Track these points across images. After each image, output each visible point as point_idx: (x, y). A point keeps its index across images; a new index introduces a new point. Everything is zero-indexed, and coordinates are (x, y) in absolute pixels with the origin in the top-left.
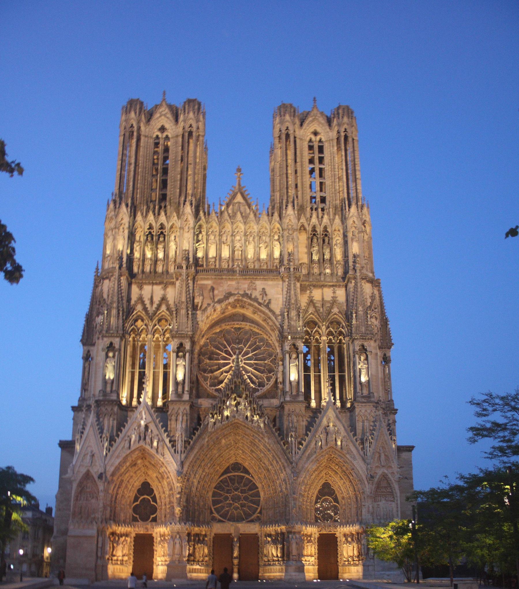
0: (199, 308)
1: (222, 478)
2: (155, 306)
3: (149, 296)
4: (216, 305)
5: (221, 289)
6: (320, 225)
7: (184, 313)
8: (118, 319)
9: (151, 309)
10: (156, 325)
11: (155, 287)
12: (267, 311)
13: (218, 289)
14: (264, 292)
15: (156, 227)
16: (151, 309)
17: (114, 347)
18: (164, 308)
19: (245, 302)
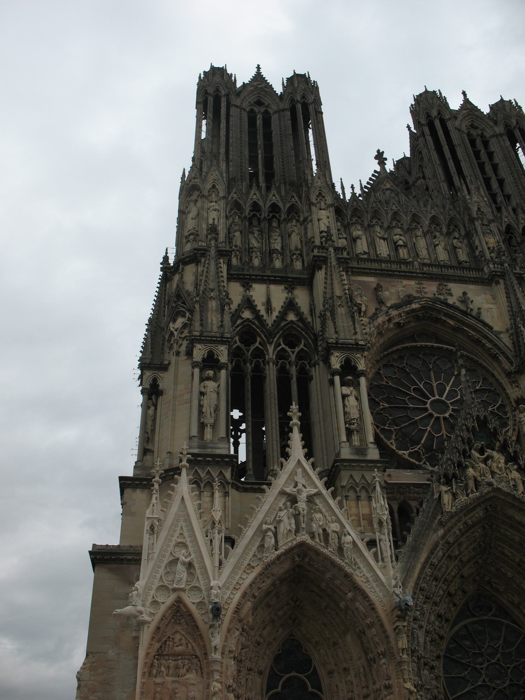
1: (457, 628)
2: (275, 314)
3: (264, 300)
4: (390, 311)
5: (393, 290)
6: (518, 225)
7: (343, 312)
8: (222, 316)
9: (270, 320)
10: (280, 345)
11: (273, 287)
13: (387, 290)
14: (464, 299)
15: (265, 207)
16: (270, 320)
17: (218, 361)
18: (291, 317)
19: (439, 311)
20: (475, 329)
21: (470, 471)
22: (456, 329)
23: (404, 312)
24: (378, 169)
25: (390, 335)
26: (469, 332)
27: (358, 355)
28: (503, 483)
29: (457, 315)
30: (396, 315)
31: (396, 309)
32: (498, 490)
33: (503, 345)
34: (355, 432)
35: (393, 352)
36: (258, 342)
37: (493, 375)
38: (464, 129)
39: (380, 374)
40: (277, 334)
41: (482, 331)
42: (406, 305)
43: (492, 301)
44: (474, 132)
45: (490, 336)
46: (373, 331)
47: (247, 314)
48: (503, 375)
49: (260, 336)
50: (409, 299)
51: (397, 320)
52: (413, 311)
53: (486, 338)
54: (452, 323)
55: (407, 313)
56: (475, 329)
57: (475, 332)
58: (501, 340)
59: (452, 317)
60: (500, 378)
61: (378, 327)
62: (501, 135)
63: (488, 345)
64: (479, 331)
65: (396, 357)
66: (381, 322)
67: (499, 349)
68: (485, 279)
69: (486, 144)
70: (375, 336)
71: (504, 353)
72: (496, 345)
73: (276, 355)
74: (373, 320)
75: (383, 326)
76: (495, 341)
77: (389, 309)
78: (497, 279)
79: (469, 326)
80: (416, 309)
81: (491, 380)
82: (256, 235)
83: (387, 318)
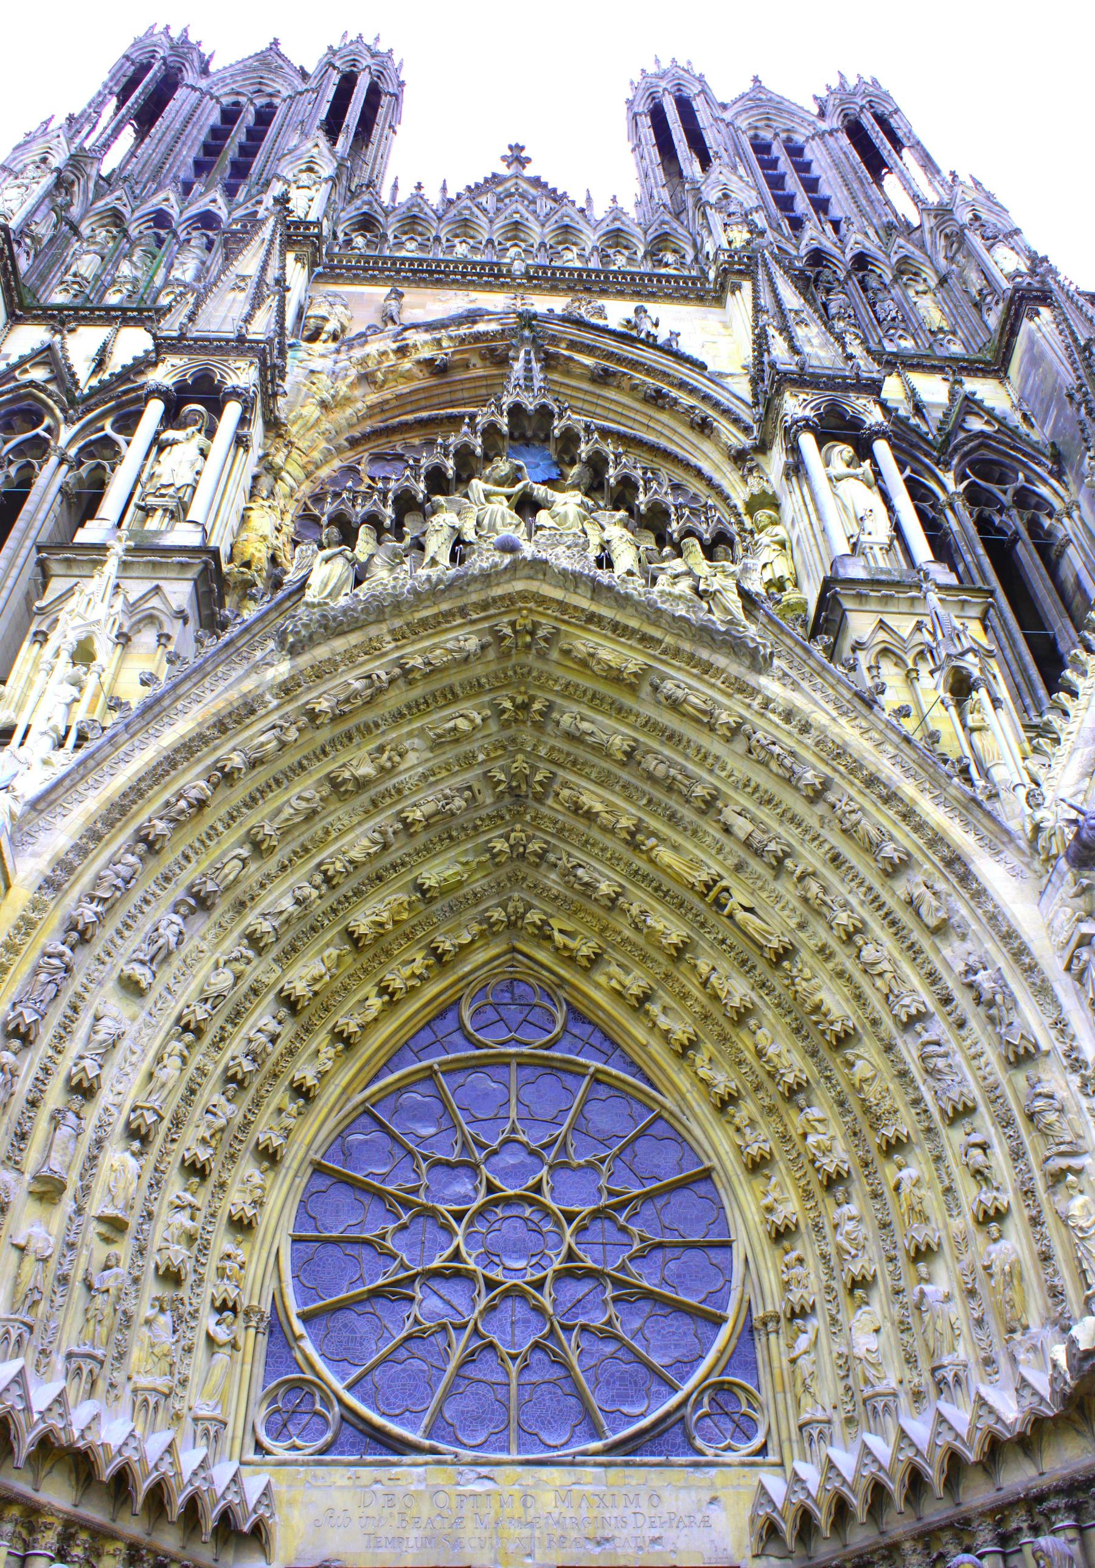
0: (324, 336)
12: (666, 363)
20: (650, 371)
21: (445, 519)
22: (602, 378)
23: (450, 338)
24: (503, 170)
25: (404, 388)
26: (631, 378)
27: (238, 364)
28: (560, 549)
29: (606, 344)
30: (426, 342)
31: (426, 331)
32: (539, 566)
33: (727, 395)
34: (160, 512)
35: (405, 427)
36: (43, 426)
37: (699, 473)
38: (743, 123)
39: (358, 472)
40: (97, 405)
41: (671, 372)
42: (461, 324)
43: (723, 331)
44: (767, 135)
45: (691, 381)
46: (346, 369)
47: (39, 374)
48: (727, 467)
49: (53, 415)
50: (472, 316)
51: (426, 353)
52: (478, 337)
53: (682, 385)
54: (588, 361)
55: (462, 340)
56: (650, 371)
57: (653, 378)
58: (723, 388)
59: (590, 350)
60: (717, 478)
61: (363, 362)
62: (831, 133)
63: (687, 400)
64: (665, 374)
65: (416, 442)
66: (374, 353)
67: (716, 405)
68: (708, 291)
69: (795, 151)
70: (349, 380)
71: (726, 412)
72: (706, 398)
73: (81, 449)
74: (351, 347)
75: (379, 363)
76: (704, 389)
77: (406, 329)
78: (733, 279)
79: (635, 365)
80: (486, 333)
81: (695, 486)
82: (135, 259)
83: (394, 346)
